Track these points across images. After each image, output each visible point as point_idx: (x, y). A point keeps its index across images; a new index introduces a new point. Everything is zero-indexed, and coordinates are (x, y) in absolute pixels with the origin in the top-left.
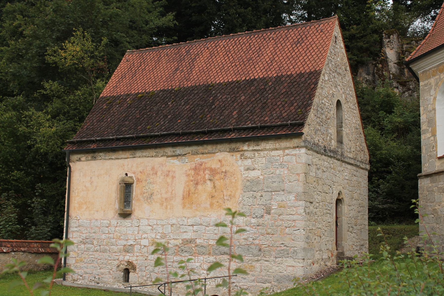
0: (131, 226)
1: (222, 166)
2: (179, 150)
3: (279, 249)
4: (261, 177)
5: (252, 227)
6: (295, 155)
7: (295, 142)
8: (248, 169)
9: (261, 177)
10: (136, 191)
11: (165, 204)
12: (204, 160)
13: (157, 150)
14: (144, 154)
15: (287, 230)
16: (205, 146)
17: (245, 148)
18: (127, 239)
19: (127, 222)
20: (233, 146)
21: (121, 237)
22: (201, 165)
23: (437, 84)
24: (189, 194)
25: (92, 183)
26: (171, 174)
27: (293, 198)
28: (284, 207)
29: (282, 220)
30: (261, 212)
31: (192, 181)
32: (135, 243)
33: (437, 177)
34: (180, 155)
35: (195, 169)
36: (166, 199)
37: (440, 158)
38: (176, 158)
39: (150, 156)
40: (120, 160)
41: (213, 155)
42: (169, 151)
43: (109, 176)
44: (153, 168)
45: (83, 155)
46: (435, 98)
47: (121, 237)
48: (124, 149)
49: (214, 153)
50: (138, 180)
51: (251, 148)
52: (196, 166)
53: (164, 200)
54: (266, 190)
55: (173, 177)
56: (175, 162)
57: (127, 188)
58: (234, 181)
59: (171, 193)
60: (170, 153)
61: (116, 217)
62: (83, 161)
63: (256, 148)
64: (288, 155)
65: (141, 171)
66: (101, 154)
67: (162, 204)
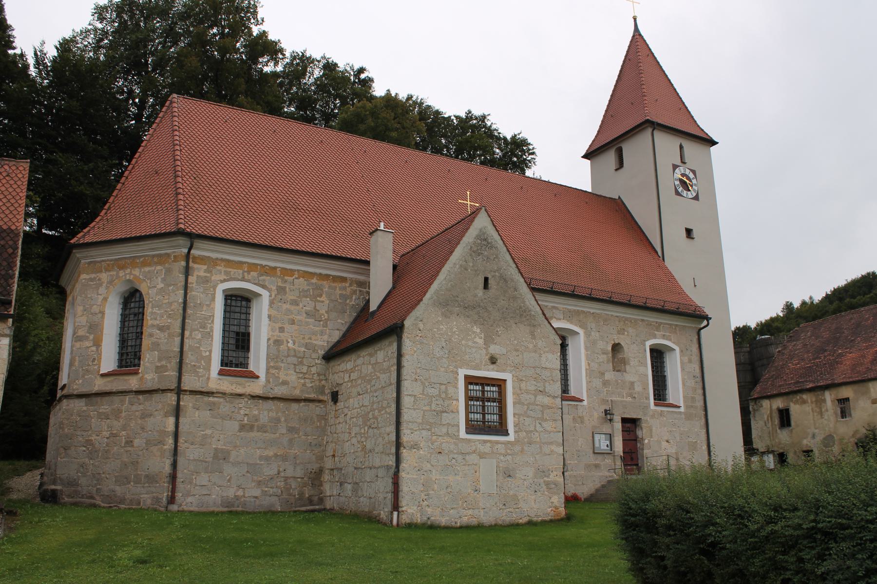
23: (111, 282)
33: (99, 399)
37: (103, 375)
46: (105, 299)
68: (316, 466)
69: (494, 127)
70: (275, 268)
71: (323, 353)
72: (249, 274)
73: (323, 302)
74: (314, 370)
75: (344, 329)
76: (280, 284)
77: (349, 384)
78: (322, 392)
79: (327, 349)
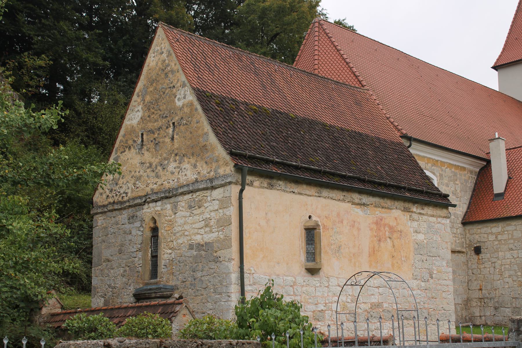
0: (321, 286)
1: (398, 224)
2: (365, 199)
3: (440, 312)
4: (425, 241)
5: (421, 291)
6: (443, 224)
7: (443, 212)
8: (416, 232)
9: (425, 241)
10: (325, 239)
11: (353, 260)
12: (383, 215)
13: (344, 194)
14: (331, 195)
15: (444, 295)
16: (386, 200)
17: (414, 209)
18: (316, 303)
19: (314, 280)
20: (407, 205)
21: (310, 301)
22: (381, 220)
24: (374, 251)
25: (268, 221)
26: (356, 225)
27: (445, 265)
28: (441, 273)
29: (440, 285)
30: (427, 276)
31: (375, 236)
32: (325, 309)
34: (364, 204)
35: (377, 223)
36: (354, 255)
38: (359, 206)
39: (336, 198)
40: (301, 196)
41: (390, 211)
42: (356, 197)
43: (290, 215)
44: (338, 215)
45: (257, 179)
47: (310, 301)
48: (309, 183)
49: (392, 209)
50: (324, 226)
51: (418, 211)
52: (377, 221)
53: (352, 256)
54: (429, 255)
55: (359, 229)
56: (358, 211)
57: (311, 234)
58: (407, 242)
59: (359, 247)
60: (357, 201)
61: (303, 273)
62: (255, 187)
63: (422, 211)
64: (439, 223)
65: (327, 215)
66: (281, 183)
67: (350, 260)
68: (465, 297)
69: (324, 12)
70: (437, 161)
71: (461, 219)
72: (427, 163)
73: (458, 184)
74: (458, 230)
75: (468, 203)
76: (440, 172)
77: (497, 243)
78: (463, 247)
79: (462, 216)
